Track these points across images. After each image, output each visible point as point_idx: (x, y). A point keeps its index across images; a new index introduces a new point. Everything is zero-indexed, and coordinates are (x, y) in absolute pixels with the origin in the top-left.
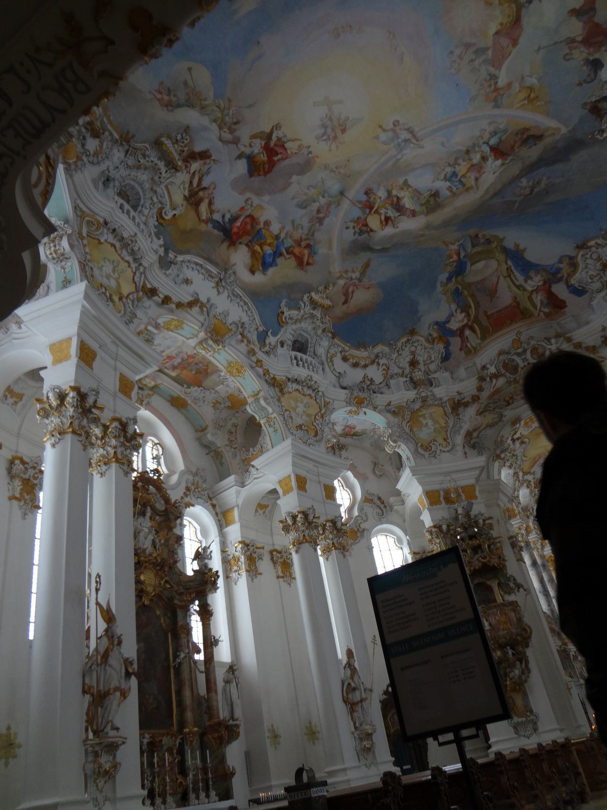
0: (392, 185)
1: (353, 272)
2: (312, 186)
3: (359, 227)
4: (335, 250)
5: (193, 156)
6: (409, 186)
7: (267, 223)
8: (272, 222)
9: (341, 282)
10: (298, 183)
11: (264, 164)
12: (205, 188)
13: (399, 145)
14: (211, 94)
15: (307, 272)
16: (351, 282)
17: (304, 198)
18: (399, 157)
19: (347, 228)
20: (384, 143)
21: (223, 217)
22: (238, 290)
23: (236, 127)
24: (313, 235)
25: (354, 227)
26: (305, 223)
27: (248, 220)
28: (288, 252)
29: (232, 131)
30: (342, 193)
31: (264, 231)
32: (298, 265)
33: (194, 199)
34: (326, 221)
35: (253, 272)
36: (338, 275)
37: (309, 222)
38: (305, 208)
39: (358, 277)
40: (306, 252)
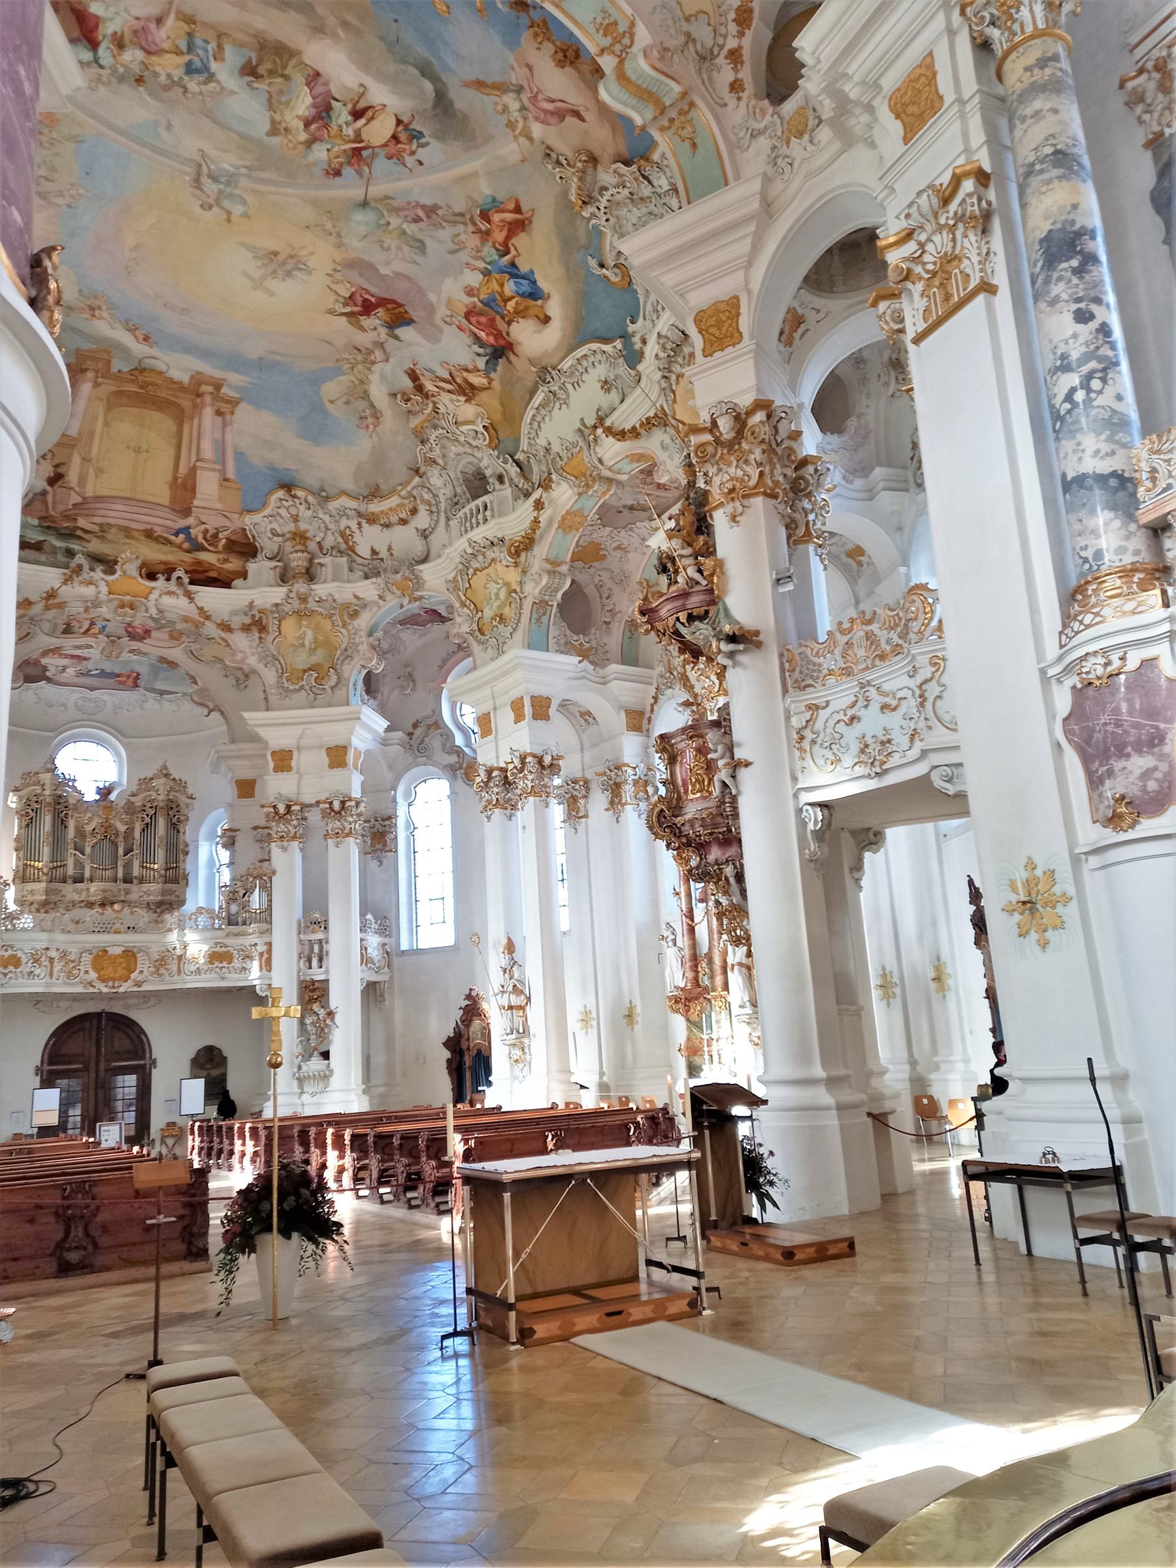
0: (295, 148)
1: (506, 109)
2: (382, 246)
3: (407, 147)
4: (475, 164)
5: (419, 388)
6: (273, 122)
7: (470, 292)
8: (466, 284)
9: (537, 129)
10: (389, 263)
11: (388, 309)
12: (451, 374)
13: (228, 184)
14: (343, 378)
15: (533, 210)
16: (531, 107)
17: (406, 249)
18: (243, 171)
19: (421, 163)
20: (244, 202)
21: (479, 355)
22: (566, 365)
23: (364, 351)
24: (461, 215)
25: (413, 153)
26: (446, 233)
27: (473, 320)
28: (507, 252)
29: (372, 351)
30: (364, 204)
31: (482, 296)
32: (523, 230)
33: (468, 391)
34: (427, 201)
35: (546, 320)
36: (522, 140)
37: (443, 228)
38: (421, 241)
39: (512, 95)
40: (496, 218)
